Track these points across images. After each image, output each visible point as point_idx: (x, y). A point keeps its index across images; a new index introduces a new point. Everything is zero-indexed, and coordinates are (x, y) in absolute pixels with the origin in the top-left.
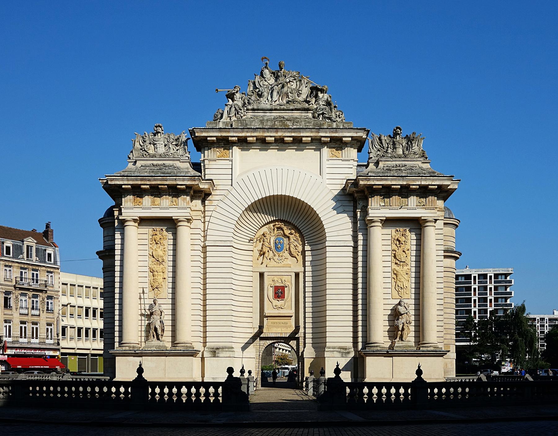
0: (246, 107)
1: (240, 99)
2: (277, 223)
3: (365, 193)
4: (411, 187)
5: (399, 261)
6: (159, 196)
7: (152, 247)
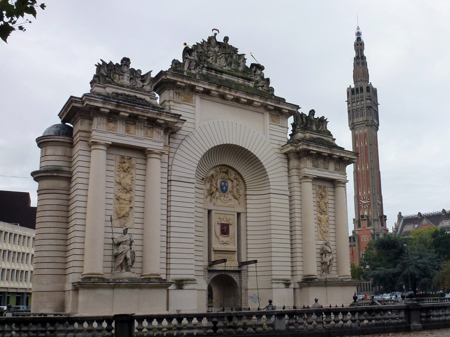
0: (202, 64)
2: (223, 168)
7: (119, 174)
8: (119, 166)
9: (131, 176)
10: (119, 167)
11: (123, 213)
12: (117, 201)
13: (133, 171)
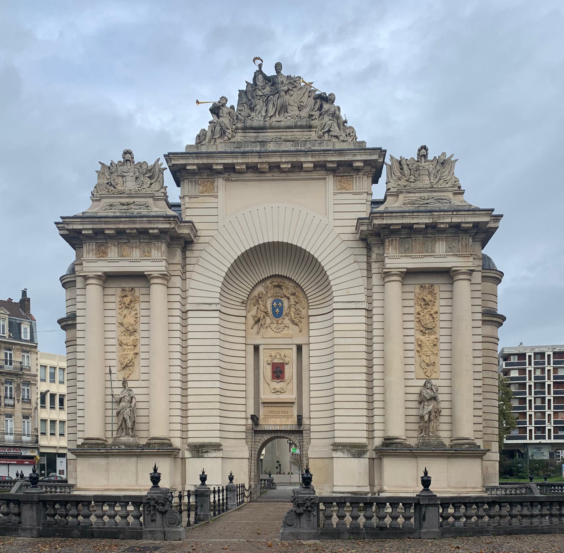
0: (235, 125)
1: (228, 115)
3: (380, 237)
4: (439, 226)
5: (425, 328)
7: (120, 312)
9: (133, 313)
10: (120, 303)
11: (126, 361)
13: (137, 306)
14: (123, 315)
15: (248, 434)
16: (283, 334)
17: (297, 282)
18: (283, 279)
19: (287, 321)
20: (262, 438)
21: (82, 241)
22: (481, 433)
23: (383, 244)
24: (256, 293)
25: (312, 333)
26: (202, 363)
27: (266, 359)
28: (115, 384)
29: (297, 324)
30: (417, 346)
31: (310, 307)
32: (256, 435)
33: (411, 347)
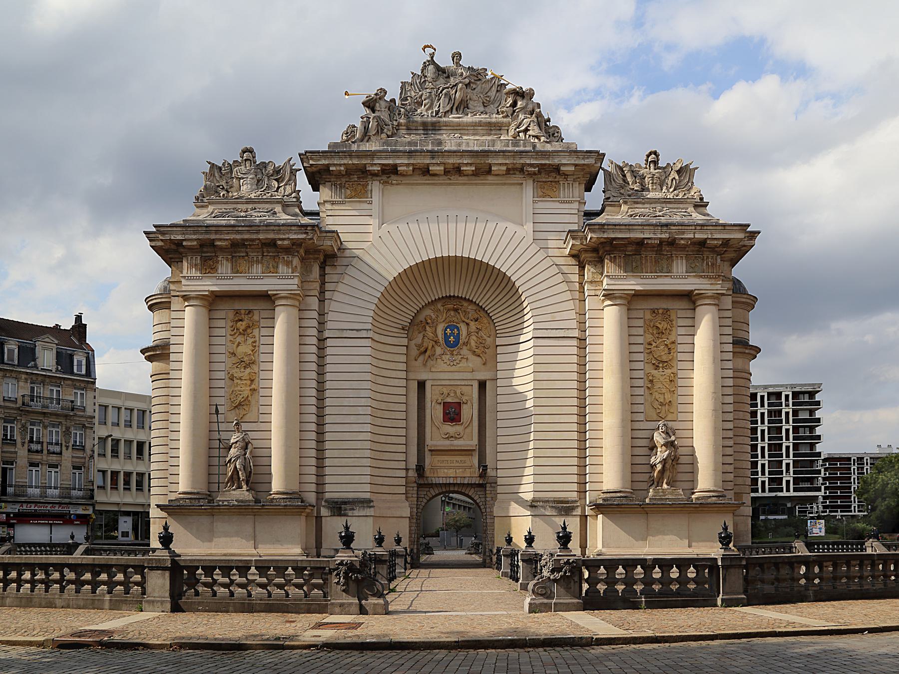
0: (397, 120)
1: (387, 110)
3: (598, 253)
6: (246, 258)
7: (232, 340)
8: (233, 326)
9: (250, 341)
10: (232, 329)
11: (240, 398)
12: (229, 382)
13: (256, 332)
14: (236, 344)
15: (408, 488)
16: (460, 367)
17: (480, 304)
18: (461, 301)
19: (465, 351)
20: (428, 493)
21: (181, 254)
22: (732, 483)
23: (601, 261)
24: (421, 317)
25: (499, 366)
26: (346, 402)
27: (435, 397)
28: (223, 427)
29: (479, 356)
30: (647, 382)
31: (498, 335)
32: (420, 489)
33: (640, 383)
